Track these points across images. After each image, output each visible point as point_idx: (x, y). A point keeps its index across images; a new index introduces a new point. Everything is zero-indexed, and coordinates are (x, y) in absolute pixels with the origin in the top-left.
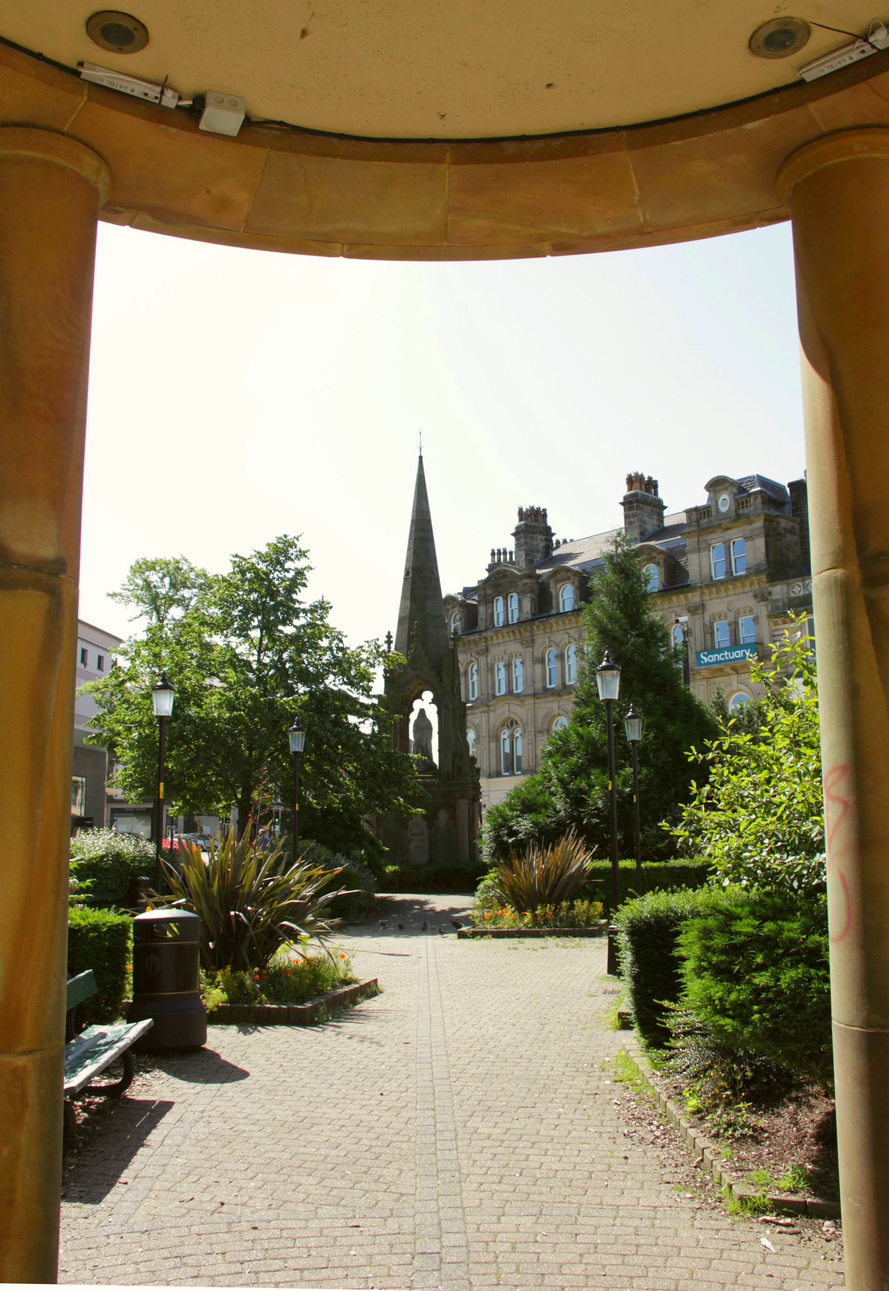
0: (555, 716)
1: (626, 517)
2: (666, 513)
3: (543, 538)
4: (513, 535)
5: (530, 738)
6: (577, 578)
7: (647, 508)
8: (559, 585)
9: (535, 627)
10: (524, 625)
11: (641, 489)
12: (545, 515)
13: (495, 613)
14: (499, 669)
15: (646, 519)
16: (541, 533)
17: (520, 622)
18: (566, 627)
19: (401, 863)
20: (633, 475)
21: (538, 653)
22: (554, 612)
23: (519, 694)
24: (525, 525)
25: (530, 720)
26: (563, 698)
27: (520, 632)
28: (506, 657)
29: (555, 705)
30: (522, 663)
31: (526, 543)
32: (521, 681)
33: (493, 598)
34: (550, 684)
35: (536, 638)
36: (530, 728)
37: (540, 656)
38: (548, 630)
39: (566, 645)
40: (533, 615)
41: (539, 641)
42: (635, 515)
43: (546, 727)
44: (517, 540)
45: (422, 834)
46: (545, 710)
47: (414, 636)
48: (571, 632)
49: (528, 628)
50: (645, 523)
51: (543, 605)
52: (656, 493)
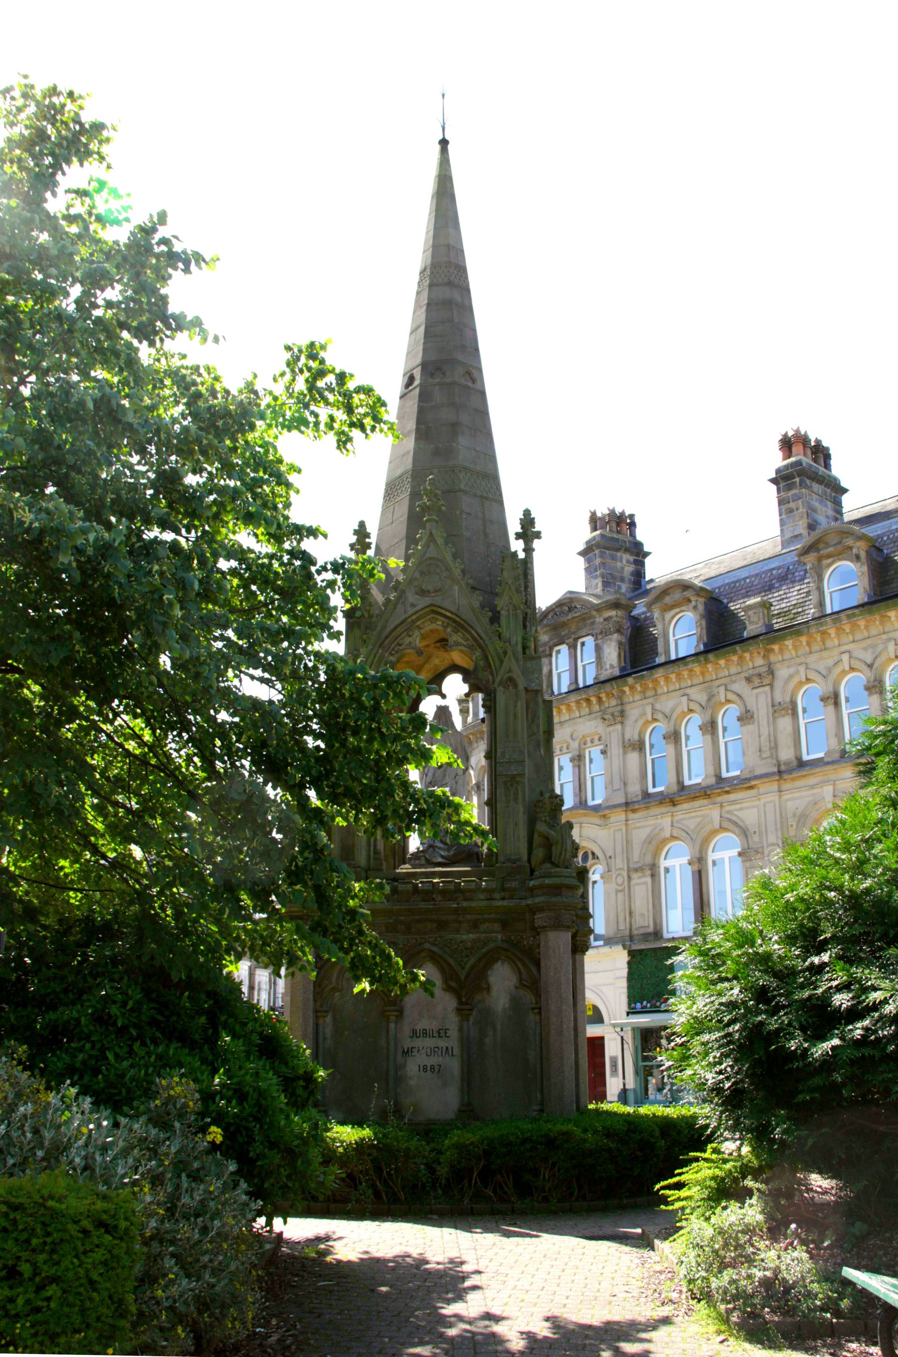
0: (665, 841)
1: (781, 502)
2: (845, 499)
3: (631, 558)
4: (583, 553)
5: (620, 880)
6: (702, 600)
7: (816, 487)
8: (668, 616)
9: (626, 689)
10: (608, 685)
11: (805, 455)
12: (632, 525)
13: (555, 673)
14: (561, 768)
15: (817, 504)
16: (627, 550)
17: (600, 683)
18: (683, 685)
19: (380, 1120)
20: (790, 434)
21: (631, 733)
22: (660, 659)
23: (600, 805)
24: (602, 536)
25: (619, 848)
26: (678, 808)
27: (600, 699)
28: (575, 745)
29: (667, 820)
30: (603, 752)
31: (603, 564)
32: (600, 784)
33: (551, 649)
34: (654, 786)
35: (627, 708)
36: (620, 862)
37: (636, 737)
38: (650, 693)
39: (684, 714)
40: (622, 669)
41: (633, 712)
42: (796, 498)
43: (648, 860)
44: (588, 561)
45: (442, 1033)
46: (648, 830)
47: (425, 509)
48: (695, 693)
49: (615, 692)
50: (814, 510)
51: (640, 653)
52: (827, 466)
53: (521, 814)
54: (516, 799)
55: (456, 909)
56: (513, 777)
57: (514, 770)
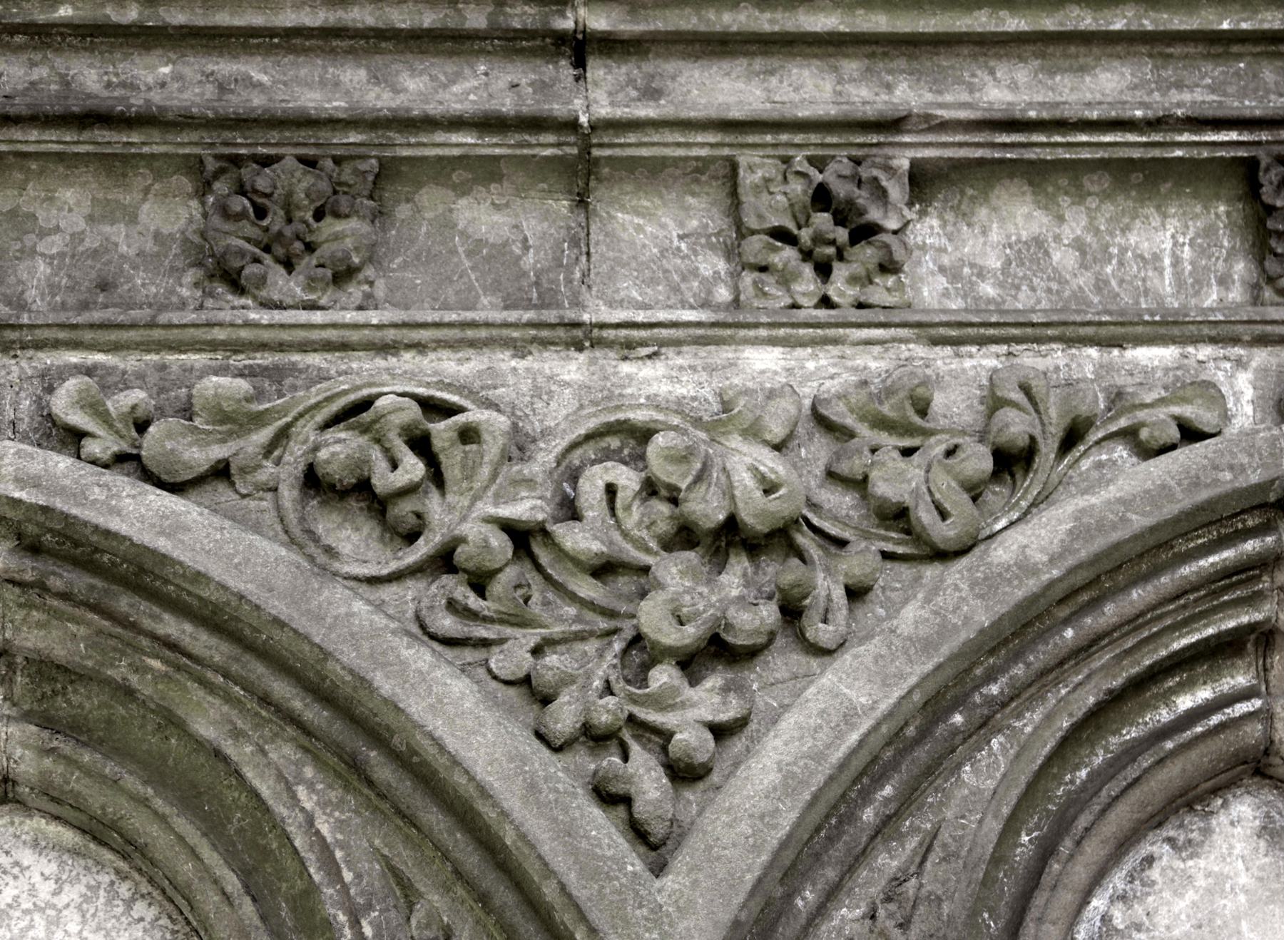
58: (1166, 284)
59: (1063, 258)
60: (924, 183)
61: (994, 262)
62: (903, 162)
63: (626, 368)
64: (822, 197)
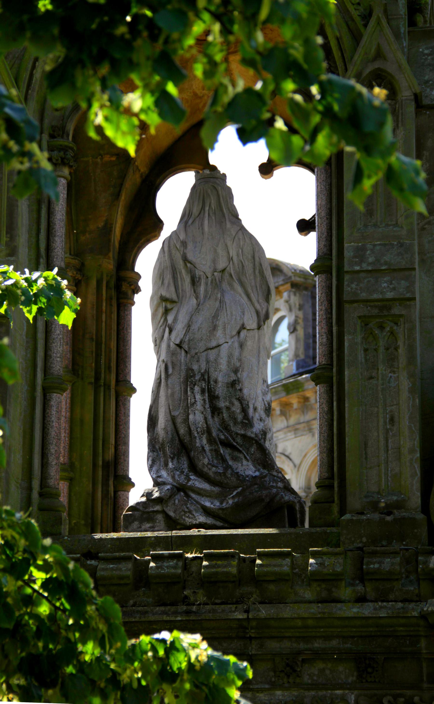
53: (405, 395)
54: (391, 360)
55: (242, 626)
56: (385, 305)
57: (386, 289)
58: (343, 677)
59: (328, 672)
60: (303, 661)
61: (316, 673)
62: (300, 659)
63: (258, 694)
64: (288, 665)
